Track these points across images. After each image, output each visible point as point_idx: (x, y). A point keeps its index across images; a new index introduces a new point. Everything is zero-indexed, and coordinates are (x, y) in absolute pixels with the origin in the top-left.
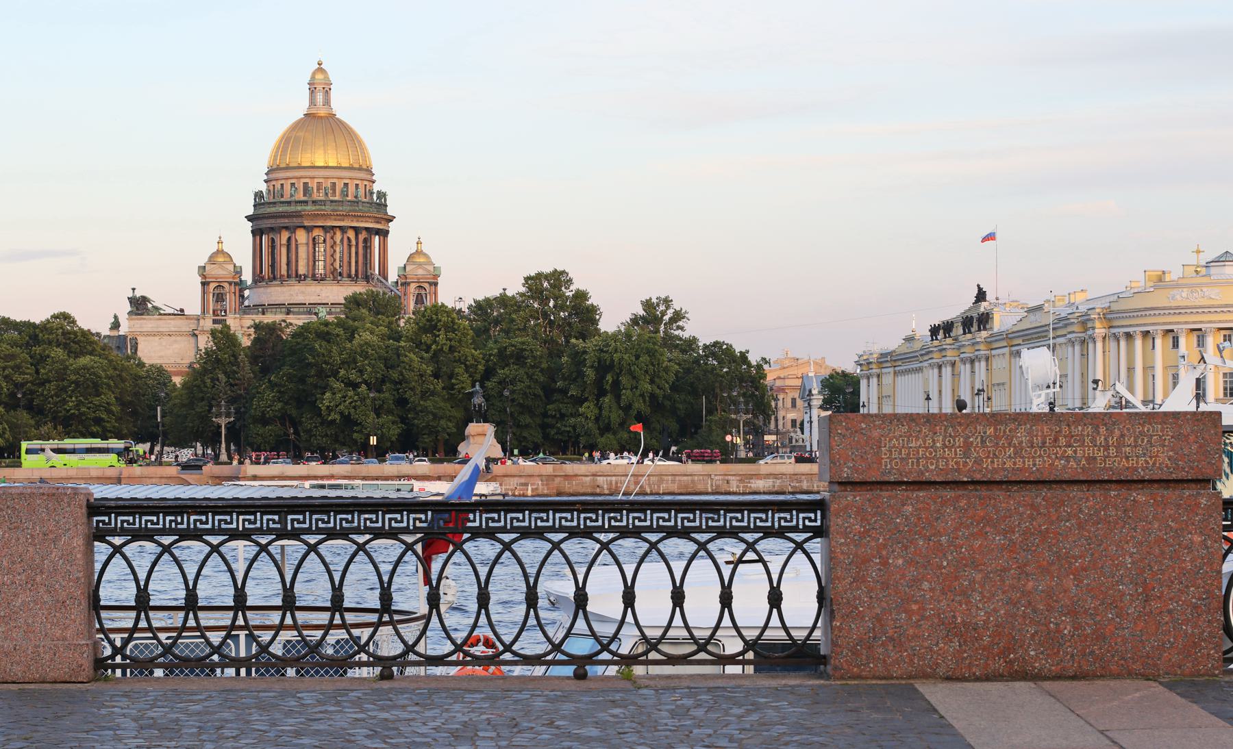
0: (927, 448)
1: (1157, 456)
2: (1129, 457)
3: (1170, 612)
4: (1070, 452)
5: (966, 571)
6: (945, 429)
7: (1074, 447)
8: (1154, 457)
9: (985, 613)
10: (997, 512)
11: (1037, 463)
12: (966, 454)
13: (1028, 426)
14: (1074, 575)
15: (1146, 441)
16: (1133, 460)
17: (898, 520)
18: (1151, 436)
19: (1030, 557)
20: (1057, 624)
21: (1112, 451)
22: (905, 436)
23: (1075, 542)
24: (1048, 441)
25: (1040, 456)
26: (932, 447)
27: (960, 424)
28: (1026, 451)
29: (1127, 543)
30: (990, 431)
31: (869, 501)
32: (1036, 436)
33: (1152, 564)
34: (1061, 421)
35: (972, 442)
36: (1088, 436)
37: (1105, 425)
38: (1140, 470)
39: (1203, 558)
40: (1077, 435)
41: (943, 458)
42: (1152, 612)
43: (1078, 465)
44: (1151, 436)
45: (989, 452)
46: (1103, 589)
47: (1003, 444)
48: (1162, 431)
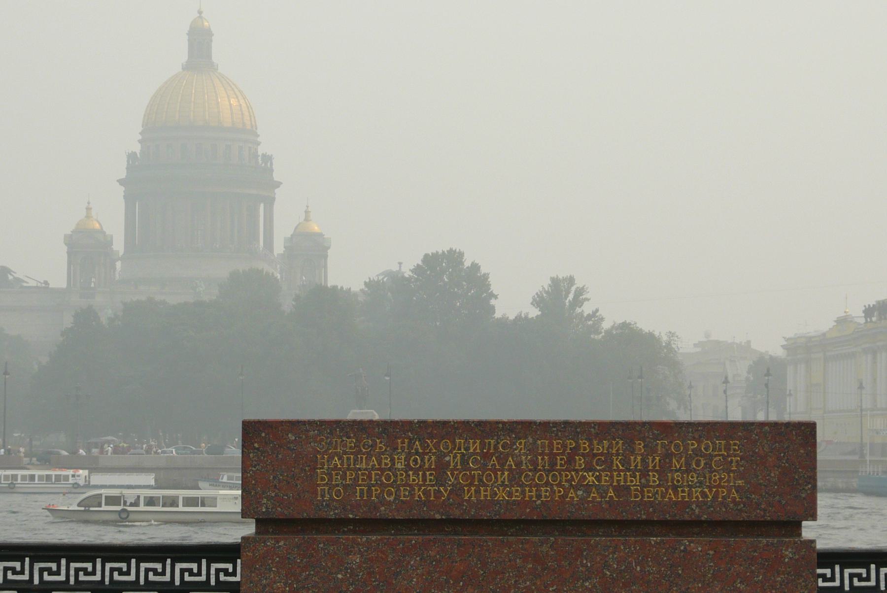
1: (719, 486)
2: (678, 487)
4: (590, 478)
6: (410, 443)
8: (715, 486)
11: (543, 494)
12: (440, 480)
13: (531, 440)
16: (683, 491)
17: (340, 576)
21: (654, 478)
22: (352, 453)
24: (559, 462)
25: (547, 484)
26: (389, 469)
27: (431, 437)
28: (527, 475)
30: (475, 446)
32: (542, 454)
34: (578, 433)
35: (449, 462)
36: (618, 455)
38: (694, 506)
40: (602, 454)
41: (407, 485)
43: (602, 497)
48: (727, 448)
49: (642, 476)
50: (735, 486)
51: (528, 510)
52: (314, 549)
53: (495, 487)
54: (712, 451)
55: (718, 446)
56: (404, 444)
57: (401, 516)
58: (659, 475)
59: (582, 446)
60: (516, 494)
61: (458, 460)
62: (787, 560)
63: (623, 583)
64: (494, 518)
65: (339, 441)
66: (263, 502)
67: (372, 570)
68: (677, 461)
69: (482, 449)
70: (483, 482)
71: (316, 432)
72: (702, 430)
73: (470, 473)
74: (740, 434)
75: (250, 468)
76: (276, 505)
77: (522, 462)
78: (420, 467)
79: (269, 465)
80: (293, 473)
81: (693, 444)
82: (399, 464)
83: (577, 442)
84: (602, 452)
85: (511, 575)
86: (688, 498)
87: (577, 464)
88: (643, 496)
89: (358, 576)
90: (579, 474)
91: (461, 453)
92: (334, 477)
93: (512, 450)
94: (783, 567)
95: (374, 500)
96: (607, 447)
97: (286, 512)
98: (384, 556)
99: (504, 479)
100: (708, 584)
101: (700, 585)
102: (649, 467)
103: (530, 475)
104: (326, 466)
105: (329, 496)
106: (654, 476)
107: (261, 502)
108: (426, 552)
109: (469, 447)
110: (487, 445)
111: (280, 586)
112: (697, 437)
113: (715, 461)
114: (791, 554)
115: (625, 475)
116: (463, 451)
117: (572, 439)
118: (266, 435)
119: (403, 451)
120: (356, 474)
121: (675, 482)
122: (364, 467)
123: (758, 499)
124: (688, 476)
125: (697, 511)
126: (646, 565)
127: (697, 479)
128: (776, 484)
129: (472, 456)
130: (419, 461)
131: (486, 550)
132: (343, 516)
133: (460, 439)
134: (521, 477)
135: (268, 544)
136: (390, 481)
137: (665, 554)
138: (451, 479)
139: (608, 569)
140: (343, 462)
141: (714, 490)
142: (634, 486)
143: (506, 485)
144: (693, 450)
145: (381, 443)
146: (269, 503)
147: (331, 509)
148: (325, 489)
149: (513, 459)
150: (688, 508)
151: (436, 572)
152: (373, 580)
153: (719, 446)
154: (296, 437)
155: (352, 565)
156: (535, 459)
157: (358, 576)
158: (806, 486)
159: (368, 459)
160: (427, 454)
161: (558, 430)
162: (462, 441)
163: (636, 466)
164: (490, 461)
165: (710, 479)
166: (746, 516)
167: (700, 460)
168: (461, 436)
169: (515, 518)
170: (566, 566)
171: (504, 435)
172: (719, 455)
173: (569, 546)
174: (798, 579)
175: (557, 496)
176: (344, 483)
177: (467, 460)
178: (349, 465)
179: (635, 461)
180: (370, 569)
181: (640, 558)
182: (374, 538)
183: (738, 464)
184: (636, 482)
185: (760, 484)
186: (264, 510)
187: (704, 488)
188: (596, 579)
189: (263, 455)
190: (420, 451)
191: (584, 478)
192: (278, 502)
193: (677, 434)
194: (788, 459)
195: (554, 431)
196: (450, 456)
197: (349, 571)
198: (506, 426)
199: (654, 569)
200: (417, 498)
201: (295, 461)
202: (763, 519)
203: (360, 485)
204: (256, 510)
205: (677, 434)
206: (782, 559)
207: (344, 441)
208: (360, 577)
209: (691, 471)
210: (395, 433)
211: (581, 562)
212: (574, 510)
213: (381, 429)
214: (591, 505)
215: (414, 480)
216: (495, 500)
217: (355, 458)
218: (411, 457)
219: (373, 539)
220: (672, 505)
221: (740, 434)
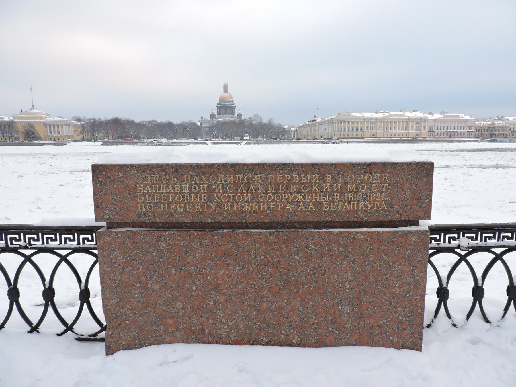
0: (176, 194)
1: (375, 201)
2: (350, 202)
3: (380, 326)
4: (299, 197)
5: (211, 294)
6: (191, 178)
7: (303, 193)
9: (229, 326)
10: (237, 247)
11: (271, 207)
12: (209, 200)
13: (264, 175)
14: (301, 297)
15: (366, 187)
17: (154, 254)
18: (371, 184)
19: (265, 283)
20: (286, 335)
24: (280, 188)
25: (274, 201)
27: (204, 174)
28: (261, 196)
29: (347, 272)
30: (230, 179)
32: (271, 183)
33: (367, 289)
34: (292, 171)
35: (215, 189)
36: (316, 184)
37: (331, 174)
38: (360, 213)
40: (306, 183)
43: (306, 208)
44: (371, 184)
45: (230, 197)
46: (325, 308)
49: (329, 196)
50: (384, 201)
51: (262, 217)
52: (138, 239)
54: (372, 180)
55: (375, 177)
56: (188, 178)
57: (188, 221)
58: (340, 195)
59: (295, 178)
60: (255, 207)
61: (220, 188)
62: (412, 242)
64: (242, 221)
65: (149, 176)
66: (107, 212)
67: (172, 250)
69: (234, 181)
70: (236, 201)
71: (135, 171)
72: (366, 168)
73: (228, 195)
74: (389, 170)
75: (98, 193)
76: (114, 214)
77: (258, 188)
78: (198, 192)
79: (109, 191)
80: (123, 196)
81: (360, 177)
82: (186, 190)
83: (291, 176)
84: (306, 182)
85: (253, 252)
86: (357, 208)
87: (291, 189)
90: (292, 195)
91: (222, 183)
92: (147, 198)
93: (252, 181)
94: (410, 246)
95: (172, 211)
96: (309, 179)
97: (120, 218)
99: (248, 198)
102: (334, 190)
103: (263, 196)
105: (145, 209)
106: (337, 195)
107: (106, 212)
108: (203, 240)
109: (227, 180)
110: (237, 179)
111: (120, 259)
112: (363, 171)
113: (373, 186)
114: (415, 239)
115: (320, 195)
116: (223, 182)
117: (289, 175)
118: (106, 174)
119: (187, 182)
120: (160, 196)
121: (349, 199)
122: (165, 192)
123: (397, 208)
124: (357, 195)
125: (361, 215)
127: (362, 197)
128: (408, 199)
129: (228, 185)
130: (197, 188)
131: (238, 239)
132: (154, 221)
133: (221, 175)
134: (258, 197)
135: (112, 236)
136: (180, 200)
137: (342, 240)
138: (217, 199)
139: (309, 249)
141: (372, 203)
142: (325, 201)
143: (249, 202)
144: (360, 180)
146: (110, 213)
147: (147, 216)
148: (142, 205)
149: (253, 186)
150: (357, 214)
151: (209, 251)
152: (173, 256)
153: (376, 177)
154: (123, 175)
155: (160, 247)
156: (266, 186)
158: (426, 200)
161: (280, 169)
162: (223, 176)
163: (326, 190)
164: (240, 188)
165: (370, 197)
166: (390, 218)
167: (364, 186)
168: (222, 173)
169: (255, 221)
170: (285, 248)
172: (376, 183)
173: (286, 236)
174: (418, 253)
175: (279, 208)
176: (153, 201)
177: (225, 188)
180: (171, 249)
181: (328, 243)
182: (173, 233)
183: (387, 188)
184: (326, 199)
185: (399, 200)
186: (108, 217)
187: (366, 202)
188: (302, 254)
189: (105, 185)
190: (198, 182)
192: (116, 212)
193: (351, 171)
194: (416, 185)
195: (278, 170)
196: (215, 185)
197: (159, 251)
198: (248, 167)
199: (336, 248)
200: (196, 210)
201: (124, 188)
202: (399, 220)
204: (103, 217)
205: (351, 171)
207: (152, 176)
208: (165, 254)
210: (182, 172)
211: (293, 245)
212: (289, 216)
213: (174, 170)
214: (299, 213)
215: (194, 200)
216: (243, 211)
217: (159, 187)
218: (192, 186)
219: (172, 233)
220: (347, 213)
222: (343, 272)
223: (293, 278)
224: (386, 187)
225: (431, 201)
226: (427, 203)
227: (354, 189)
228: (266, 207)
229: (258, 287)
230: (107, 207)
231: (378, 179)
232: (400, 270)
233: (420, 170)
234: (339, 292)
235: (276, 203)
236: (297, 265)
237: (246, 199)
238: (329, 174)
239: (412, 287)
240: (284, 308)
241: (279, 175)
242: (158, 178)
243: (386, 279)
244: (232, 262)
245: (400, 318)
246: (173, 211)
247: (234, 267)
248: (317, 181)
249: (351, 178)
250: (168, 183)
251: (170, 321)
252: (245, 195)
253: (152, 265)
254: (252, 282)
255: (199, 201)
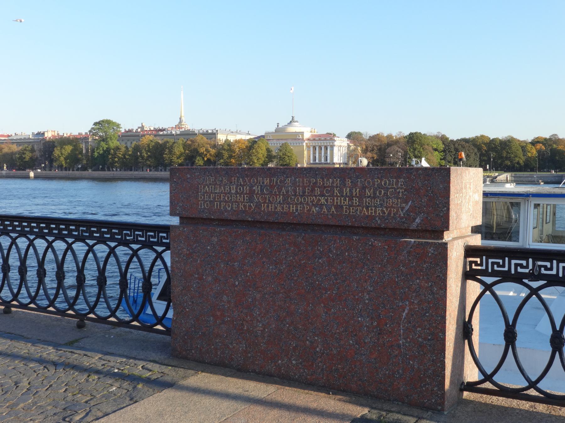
1: (392, 207)
4: (323, 200)
5: (250, 291)
7: (325, 196)
8: (389, 207)
9: (263, 325)
12: (251, 200)
13: (293, 178)
17: (209, 248)
18: (388, 189)
20: (311, 342)
21: (356, 201)
22: (213, 185)
23: (326, 276)
27: (247, 176)
28: (291, 198)
29: (366, 282)
30: (267, 181)
31: (192, 231)
32: (299, 186)
34: (317, 174)
35: (255, 190)
36: (337, 187)
37: (350, 178)
38: (377, 219)
39: (429, 303)
40: (329, 187)
41: (236, 202)
42: (384, 344)
43: (328, 211)
44: (388, 189)
46: (346, 318)
47: (275, 192)
51: (291, 218)
52: (198, 233)
53: (276, 204)
54: (388, 185)
62: (430, 255)
63: (339, 262)
68: (369, 191)
69: (270, 182)
70: (270, 201)
73: (265, 196)
77: (289, 191)
78: (242, 192)
88: (350, 212)
89: (216, 248)
98: (227, 239)
99: (280, 200)
100: (384, 266)
101: (380, 266)
104: (202, 191)
106: (356, 200)
112: (380, 177)
115: (341, 199)
123: (414, 216)
125: (379, 221)
126: (351, 252)
128: (425, 207)
130: (242, 189)
140: (209, 189)
142: (345, 205)
145: (225, 179)
157: (216, 248)
158: (443, 208)
159: (220, 187)
160: (245, 185)
162: (261, 179)
163: (346, 194)
165: (387, 202)
167: (381, 191)
171: (280, 176)
172: (392, 188)
174: (436, 267)
175: (306, 210)
178: (212, 191)
179: (346, 191)
185: (415, 207)
187: (383, 208)
190: (242, 183)
191: (319, 200)
193: (369, 175)
194: (432, 191)
200: (240, 209)
203: (216, 201)
205: (369, 175)
206: (427, 254)
209: (376, 197)
211: (317, 248)
215: (239, 199)
221: (404, 175)
222: (362, 280)
223: (317, 282)
224: (402, 192)
225: (448, 209)
226: (445, 212)
227: (372, 194)
228: (294, 209)
229: (288, 288)
230: (178, 204)
231: (394, 184)
232: (418, 284)
233: (436, 176)
234: (359, 302)
235: (303, 206)
236: (321, 269)
237: (278, 200)
238: (348, 178)
239: (431, 305)
240: (308, 312)
241: (306, 178)
242: (214, 179)
243: (404, 293)
244: (267, 261)
245: (420, 340)
246: (223, 209)
247: (268, 265)
248: (338, 185)
249: (369, 182)
250: (221, 184)
251: (219, 313)
252: (278, 196)
253: (207, 258)
254: (282, 283)
255: (242, 201)
